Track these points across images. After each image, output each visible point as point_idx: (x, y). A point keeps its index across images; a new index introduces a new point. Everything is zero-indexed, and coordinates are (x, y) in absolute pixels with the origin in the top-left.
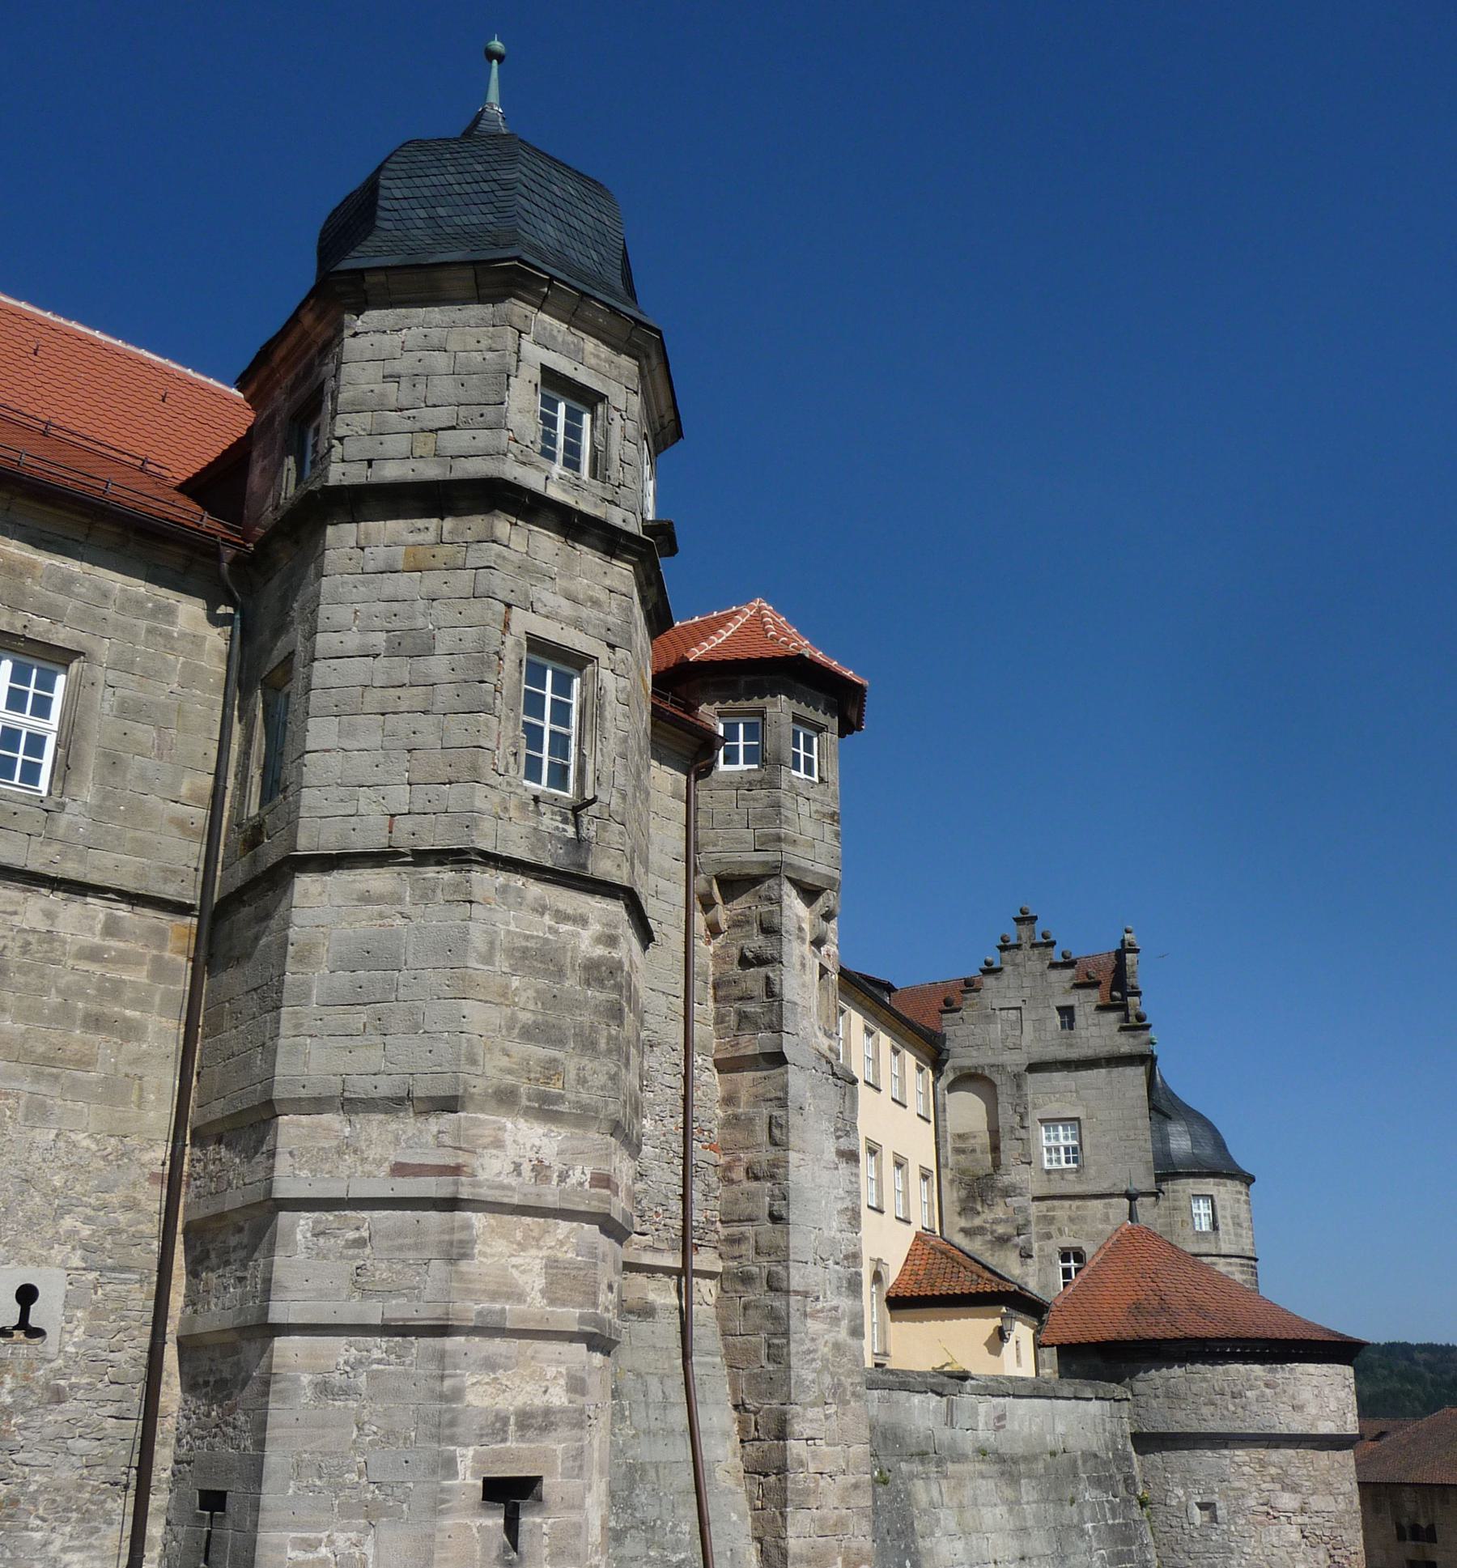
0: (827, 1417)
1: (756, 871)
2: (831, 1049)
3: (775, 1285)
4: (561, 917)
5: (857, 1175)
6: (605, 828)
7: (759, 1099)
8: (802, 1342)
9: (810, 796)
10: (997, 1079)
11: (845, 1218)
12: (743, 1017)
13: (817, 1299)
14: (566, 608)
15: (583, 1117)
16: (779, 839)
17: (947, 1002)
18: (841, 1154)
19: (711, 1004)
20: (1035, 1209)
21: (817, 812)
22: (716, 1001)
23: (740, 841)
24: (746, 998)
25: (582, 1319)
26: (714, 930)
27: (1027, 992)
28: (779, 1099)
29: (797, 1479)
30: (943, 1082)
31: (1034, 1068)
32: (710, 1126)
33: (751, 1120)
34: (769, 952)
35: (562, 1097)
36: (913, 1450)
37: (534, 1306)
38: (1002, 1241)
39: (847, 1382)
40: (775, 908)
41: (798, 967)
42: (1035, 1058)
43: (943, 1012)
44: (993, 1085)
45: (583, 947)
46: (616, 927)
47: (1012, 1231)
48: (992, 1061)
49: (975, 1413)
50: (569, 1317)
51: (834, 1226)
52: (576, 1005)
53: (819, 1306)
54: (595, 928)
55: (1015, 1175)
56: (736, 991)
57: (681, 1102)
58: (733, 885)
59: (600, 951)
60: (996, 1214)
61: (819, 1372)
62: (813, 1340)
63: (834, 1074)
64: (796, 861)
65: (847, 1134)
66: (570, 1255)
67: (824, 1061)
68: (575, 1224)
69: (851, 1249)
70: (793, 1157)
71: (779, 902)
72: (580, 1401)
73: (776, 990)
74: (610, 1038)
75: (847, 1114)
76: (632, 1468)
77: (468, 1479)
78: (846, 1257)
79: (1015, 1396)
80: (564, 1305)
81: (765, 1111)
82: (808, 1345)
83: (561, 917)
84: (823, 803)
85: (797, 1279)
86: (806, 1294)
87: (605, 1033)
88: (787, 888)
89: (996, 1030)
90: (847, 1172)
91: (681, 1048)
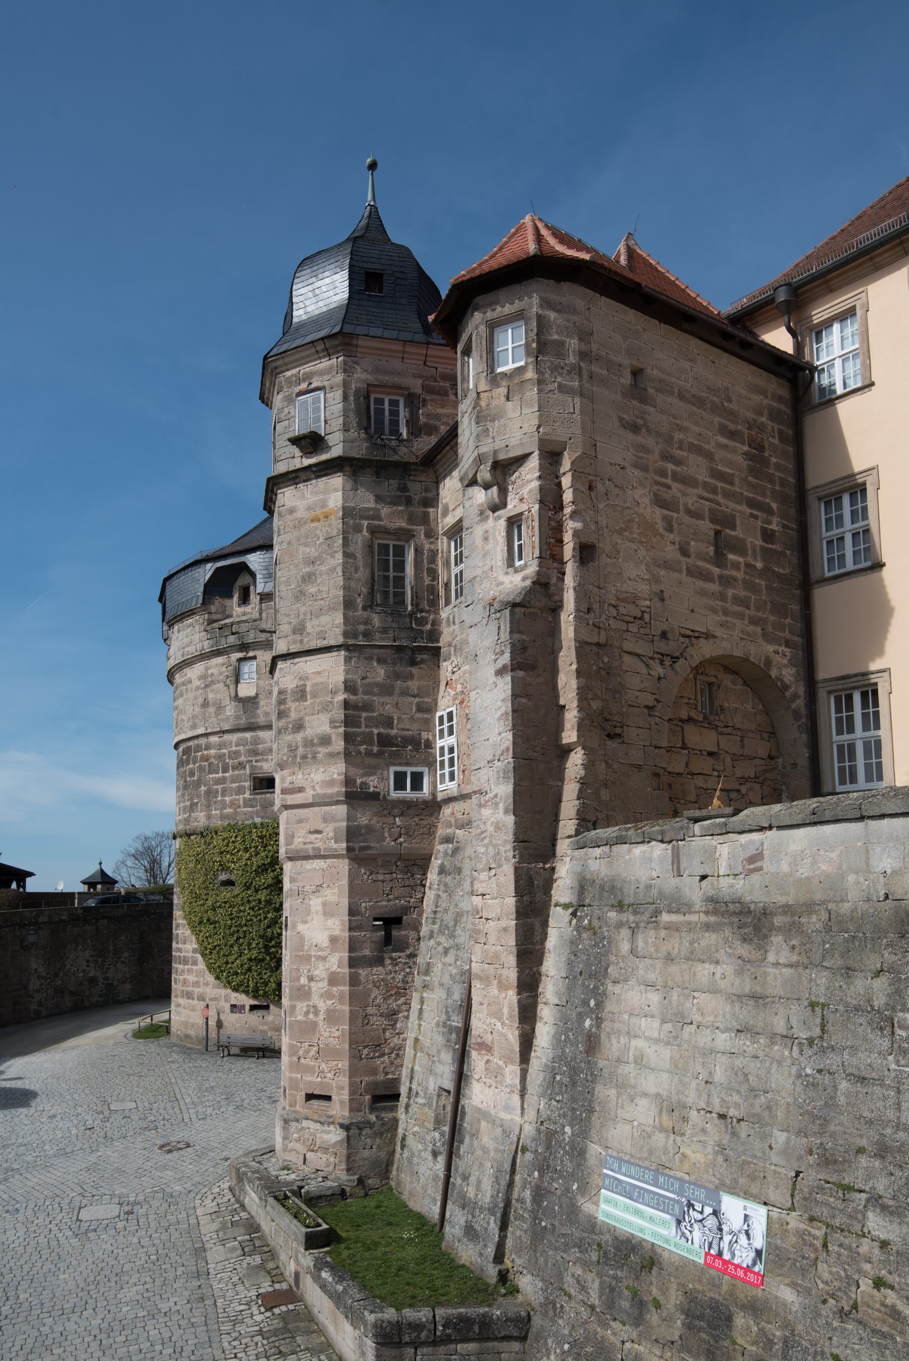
36: (631, 900)
49: (711, 856)
76: (458, 913)
79: (780, 828)
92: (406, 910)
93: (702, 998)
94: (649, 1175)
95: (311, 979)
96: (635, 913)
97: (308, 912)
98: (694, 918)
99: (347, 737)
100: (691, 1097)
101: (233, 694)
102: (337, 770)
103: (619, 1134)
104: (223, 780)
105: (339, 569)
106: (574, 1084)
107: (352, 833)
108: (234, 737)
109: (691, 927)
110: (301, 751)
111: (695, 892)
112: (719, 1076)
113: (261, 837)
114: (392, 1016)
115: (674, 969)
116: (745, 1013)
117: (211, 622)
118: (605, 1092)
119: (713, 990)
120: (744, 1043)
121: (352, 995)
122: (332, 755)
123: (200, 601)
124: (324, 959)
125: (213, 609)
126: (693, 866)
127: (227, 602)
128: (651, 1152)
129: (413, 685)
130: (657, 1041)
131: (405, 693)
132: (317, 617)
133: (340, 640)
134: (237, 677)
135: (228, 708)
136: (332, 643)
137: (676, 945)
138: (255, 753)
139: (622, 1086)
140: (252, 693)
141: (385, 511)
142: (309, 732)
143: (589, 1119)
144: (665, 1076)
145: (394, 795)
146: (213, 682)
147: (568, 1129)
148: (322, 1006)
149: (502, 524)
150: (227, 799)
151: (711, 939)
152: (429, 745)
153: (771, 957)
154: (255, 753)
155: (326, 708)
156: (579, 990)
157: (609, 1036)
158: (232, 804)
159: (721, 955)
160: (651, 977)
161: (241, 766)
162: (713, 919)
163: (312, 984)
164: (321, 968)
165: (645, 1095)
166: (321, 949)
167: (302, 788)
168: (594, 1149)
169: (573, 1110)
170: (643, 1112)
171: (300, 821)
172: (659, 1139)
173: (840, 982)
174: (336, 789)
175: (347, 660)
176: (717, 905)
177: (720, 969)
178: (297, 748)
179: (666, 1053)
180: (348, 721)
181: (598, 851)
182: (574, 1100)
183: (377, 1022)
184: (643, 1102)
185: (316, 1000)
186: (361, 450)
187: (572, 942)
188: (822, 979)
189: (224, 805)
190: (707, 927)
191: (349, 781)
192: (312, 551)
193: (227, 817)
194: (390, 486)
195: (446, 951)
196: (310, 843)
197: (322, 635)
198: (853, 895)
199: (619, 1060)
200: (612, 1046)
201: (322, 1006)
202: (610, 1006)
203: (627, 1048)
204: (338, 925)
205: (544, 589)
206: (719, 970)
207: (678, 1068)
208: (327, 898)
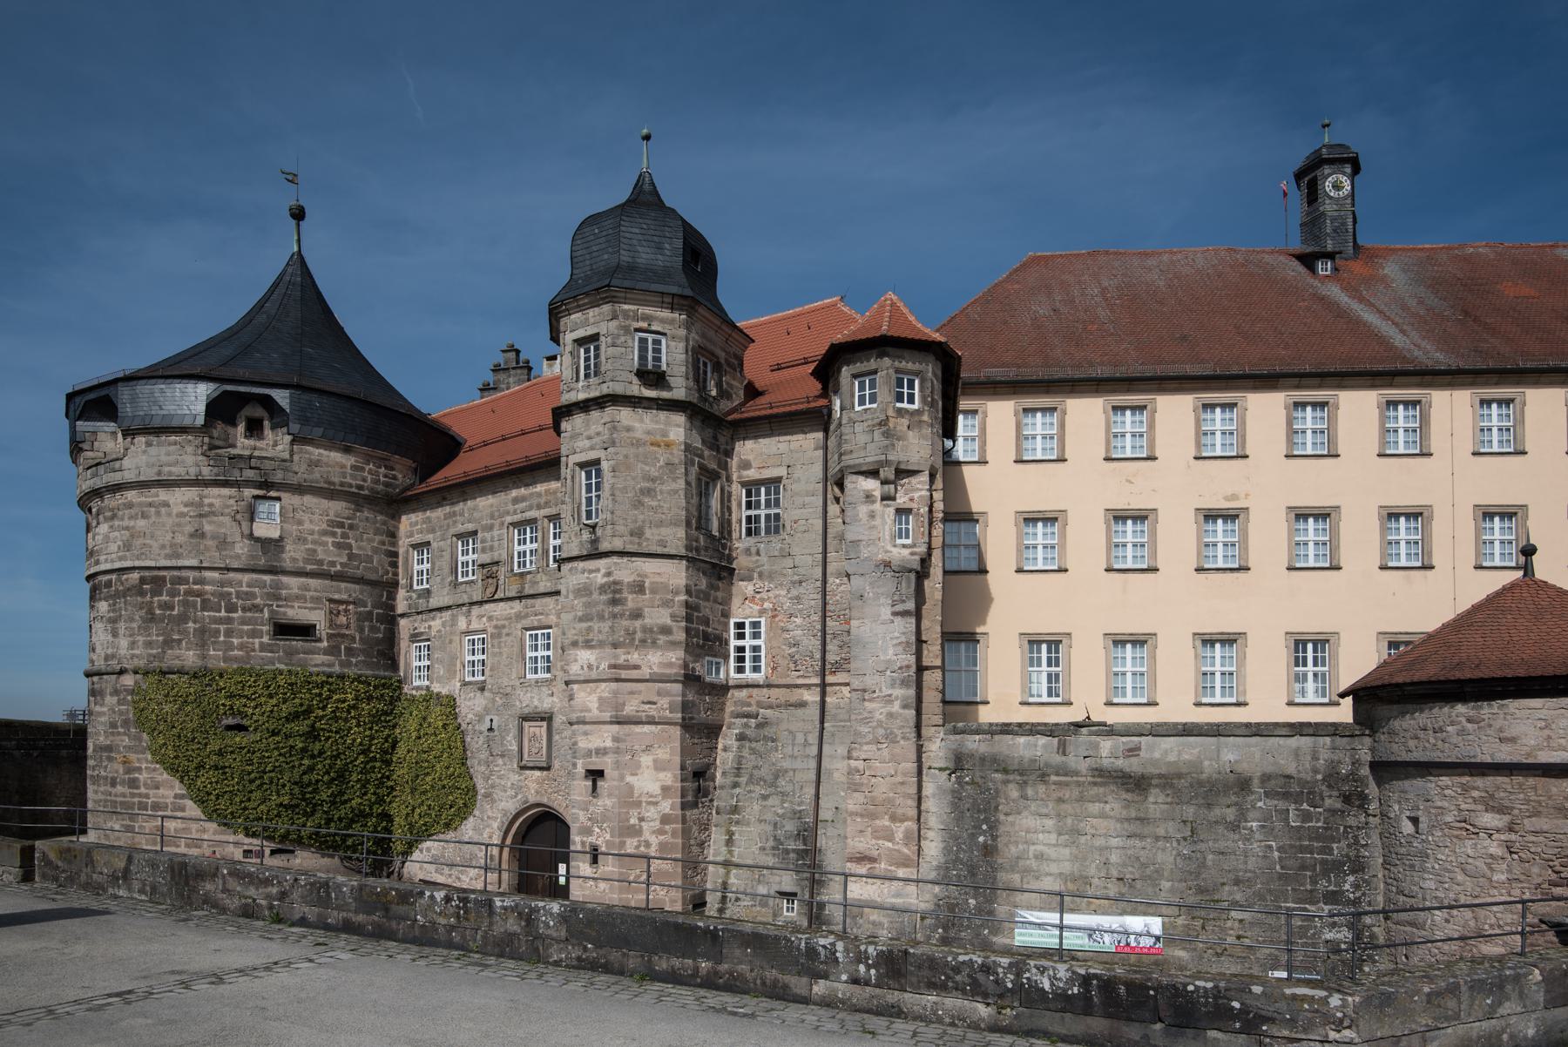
4: (591, 571)
11: (900, 648)
14: (587, 443)
15: (601, 644)
37: (595, 713)
50: (607, 716)
52: (597, 603)
77: (580, 770)
83: (591, 571)
86: (864, 691)
92: (708, 766)
97: (639, 766)
99: (688, 630)
100: (1092, 871)
101: (247, 532)
102: (676, 656)
104: (229, 620)
105: (682, 493)
107: (685, 707)
108: (246, 577)
110: (639, 635)
111: (1083, 766)
112: (1114, 858)
113: (291, 684)
114: (701, 845)
115: (1067, 808)
116: (1132, 828)
117: (212, 447)
119: (1103, 815)
121: (683, 831)
122: (674, 644)
123: (200, 421)
125: (215, 433)
127: (231, 430)
129: (720, 594)
131: (715, 601)
132: (657, 526)
133: (683, 552)
134: (252, 516)
135: (238, 546)
136: (673, 552)
138: (278, 598)
140: (276, 534)
141: (707, 453)
142: (647, 621)
145: (708, 679)
146: (214, 513)
148: (654, 840)
149: (891, 510)
150: (235, 641)
152: (727, 643)
153: (1151, 799)
154: (278, 598)
155: (666, 604)
157: (1006, 845)
158: (241, 647)
160: (1045, 811)
161: (257, 608)
168: (1001, 910)
171: (632, 693)
173: (1203, 811)
174: (675, 671)
175: (687, 568)
178: (635, 632)
180: (688, 619)
183: (695, 849)
185: (647, 835)
186: (694, 399)
187: (953, 791)
189: (230, 647)
191: (686, 666)
192: (654, 472)
193: (236, 659)
194: (709, 432)
195: (765, 797)
197: (663, 543)
201: (654, 840)
202: (1002, 829)
203: (1026, 851)
204: (670, 777)
205: (925, 561)
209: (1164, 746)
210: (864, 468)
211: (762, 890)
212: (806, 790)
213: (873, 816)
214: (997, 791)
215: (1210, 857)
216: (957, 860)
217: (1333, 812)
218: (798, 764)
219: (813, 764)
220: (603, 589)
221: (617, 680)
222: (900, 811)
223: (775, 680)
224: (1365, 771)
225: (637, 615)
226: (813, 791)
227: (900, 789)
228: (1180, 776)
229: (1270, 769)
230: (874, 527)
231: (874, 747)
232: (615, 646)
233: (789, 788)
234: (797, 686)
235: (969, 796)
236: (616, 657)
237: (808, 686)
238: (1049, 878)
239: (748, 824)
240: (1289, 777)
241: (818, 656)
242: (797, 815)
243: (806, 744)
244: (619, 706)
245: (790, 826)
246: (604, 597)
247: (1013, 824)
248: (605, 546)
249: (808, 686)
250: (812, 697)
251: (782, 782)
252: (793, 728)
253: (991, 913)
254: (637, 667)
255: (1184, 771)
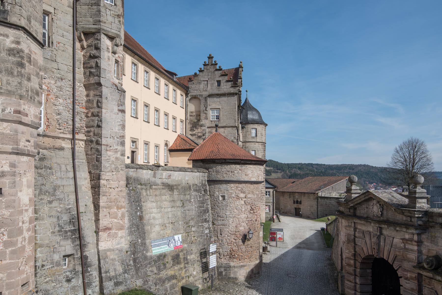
0: (113, 175)
1: (93, 31)
2: (119, 83)
3: (98, 143)
5: (124, 116)
6: (13, 8)
7: (95, 95)
8: (106, 157)
9: (111, 9)
10: (201, 98)
11: (120, 127)
12: (90, 72)
13: (111, 147)
15: (9, 93)
16: (100, 21)
17: (190, 79)
18: (119, 110)
19: (82, 69)
20: (207, 130)
21: (113, 14)
22: (84, 68)
23: (88, 21)
24: (91, 67)
25: (13, 149)
26: (83, 48)
27: (210, 76)
28: (100, 95)
29: (102, 190)
30: (188, 99)
31: (210, 96)
32: (82, 102)
33: (93, 101)
34: (97, 54)
35: (1, 88)
38: (200, 137)
39: (119, 167)
40: (99, 42)
41: (107, 59)
42: (210, 93)
43: (189, 81)
44: (200, 100)
45: (7, 44)
46: (19, 39)
47: (202, 135)
48: (201, 94)
49: (162, 175)
51: (117, 129)
53: (111, 148)
54: (12, 38)
55: (203, 122)
56: (89, 66)
57: (72, 95)
58: (88, 34)
59: (13, 46)
60: (198, 131)
61: (111, 164)
62: (109, 156)
63: (118, 89)
64: (105, 28)
65: (122, 105)
66: (8, 132)
67: (114, 86)
68: (9, 124)
69: (122, 135)
70: (103, 111)
71: (100, 40)
72: (14, 169)
73: (99, 65)
74: (18, 72)
75: (122, 100)
78: (120, 137)
80: (6, 145)
81: (97, 98)
82: (107, 158)
84: (115, 11)
85: (104, 141)
86: (107, 145)
87: (16, 70)
88: (103, 36)
89: (202, 86)
90: (121, 115)
91: (72, 80)
93: (165, 202)
94: (161, 240)
95: (23, 223)
96: (145, 186)
98: (160, 187)
100: (166, 221)
103: (153, 235)
106: (138, 229)
109: (160, 189)
111: (159, 181)
112: (170, 216)
115: (157, 198)
118: (147, 228)
119: (166, 201)
120: (173, 209)
124: (26, 210)
126: (158, 176)
128: (160, 235)
130: (157, 213)
137: (158, 192)
139: (151, 225)
143: (145, 235)
144: (160, 220)
147: (140, 240)
149: (114, 59)
151: (164, 191)
156: (134, 206)
159: (166, 194)
160: (153, 200)
162: (164, 187)
163: (24, 225)
164: (26, 216)
165: (157, 225)
166: (26, 206)
167: (27, 114)
168: (148, 242)
169: (140, 235)
170: (157, 228)
172: (162, 232)
173: (184, 196)
176: (163, 184)
177: (166, 197)
179: (159, 215)
181: (132, 170)
182: (139, 233)
184: (157, 226)
187: (128, 194)
188: (182, 196)
190: (163, 189)
195: (50, 202)
196: (27, 147)
198: (184, 183)
199: (149, 220)
200: (146, 217)
202: (144, 208)
203: (150, 216)
206: (166, 197)
207: (162, 217)
208: (28, 178)
209: (176, 175)
210: (110, 34)
211: (56, 257)
212: (70, 197)
213: (109, 207)
214: (140, 193)
215: (187, 212)
216: (133, 224)
217: (203, 195)
218: (64, 182)
219: (72, 182)
220: (11, 52)
221: (21, 123)
222: (120, 204)
223: (48, 133)
224: (206, 183)
225: (29, 79)
226: (74, 197)
227: (121, 194)
228: (179, 185)
229: (193, 182)
230: (109, 65)
231: (110, 174)
232: (21, 97)
233: (61, 196)
234: (59, 138)
235: (133, 196)
236: (20, 105)
237: (64, 139)
238: (157, 226)
239: (43, 219)
240: (196, 185)
241: (71, 123)
242: (69, 211)
243: (67, 171)
244: (17, 142)
245: (66, 217)
246: (12, 58)
247: (146, 206)
248: (13, 19)
249: (64, 139)
250: (67, 145)
251: (58, 193)
252: (59, 162)
253: (145, 244)
254: (27, 115)
255: (180, 183)
